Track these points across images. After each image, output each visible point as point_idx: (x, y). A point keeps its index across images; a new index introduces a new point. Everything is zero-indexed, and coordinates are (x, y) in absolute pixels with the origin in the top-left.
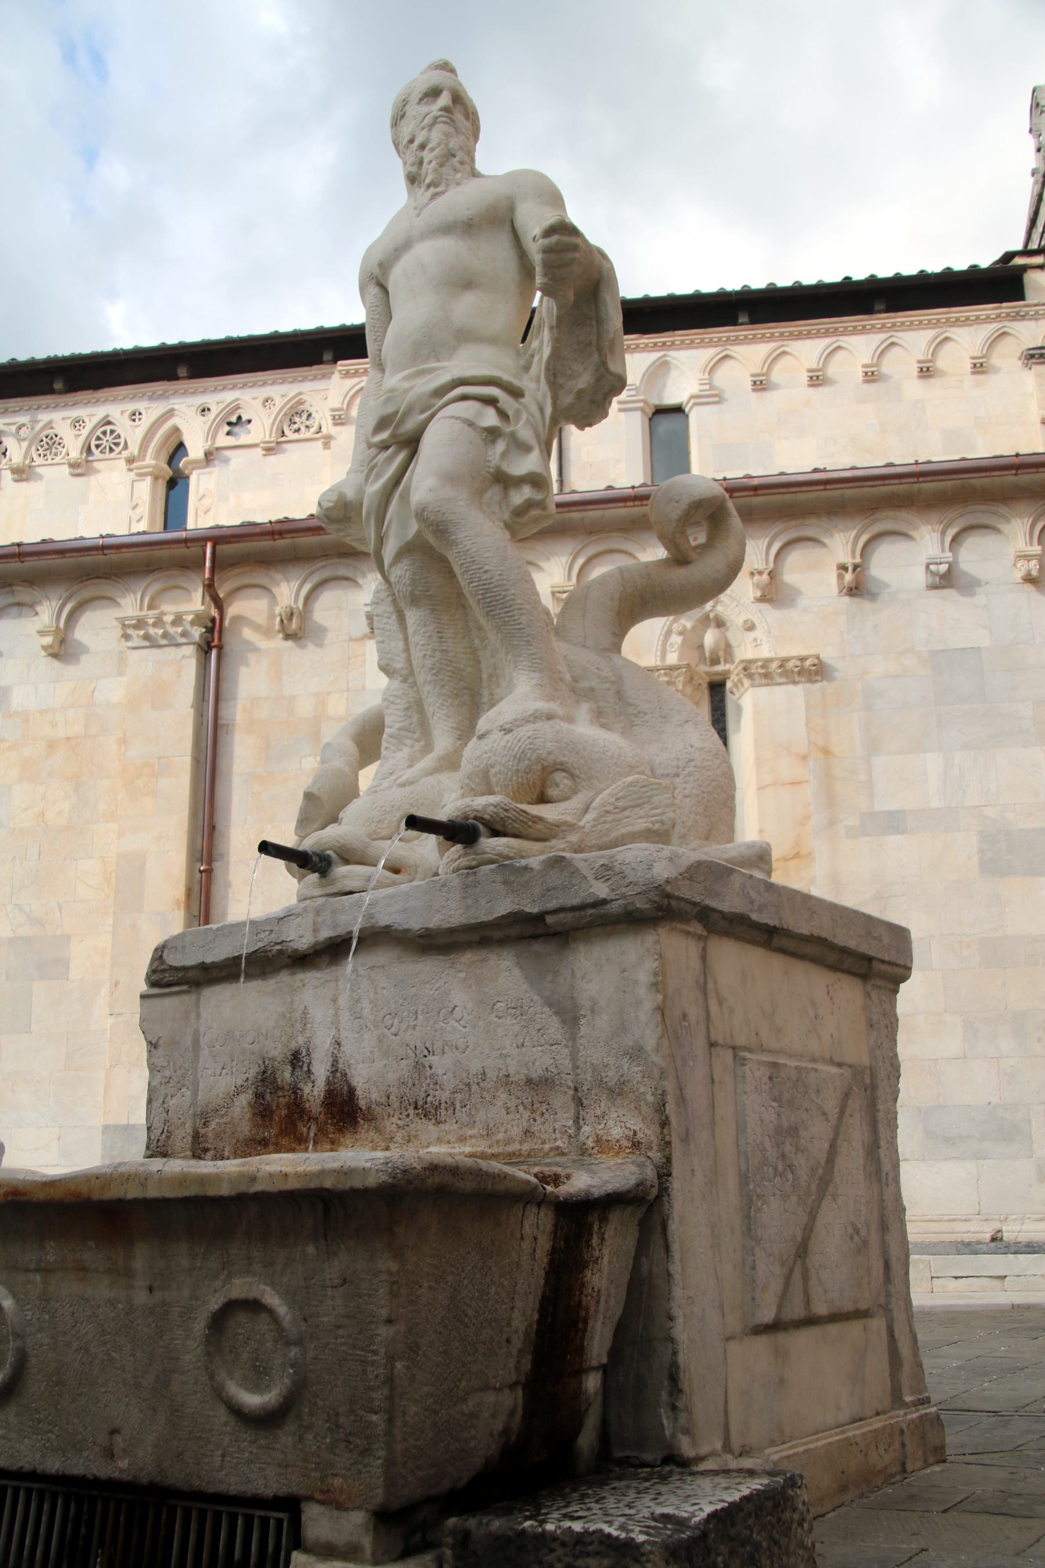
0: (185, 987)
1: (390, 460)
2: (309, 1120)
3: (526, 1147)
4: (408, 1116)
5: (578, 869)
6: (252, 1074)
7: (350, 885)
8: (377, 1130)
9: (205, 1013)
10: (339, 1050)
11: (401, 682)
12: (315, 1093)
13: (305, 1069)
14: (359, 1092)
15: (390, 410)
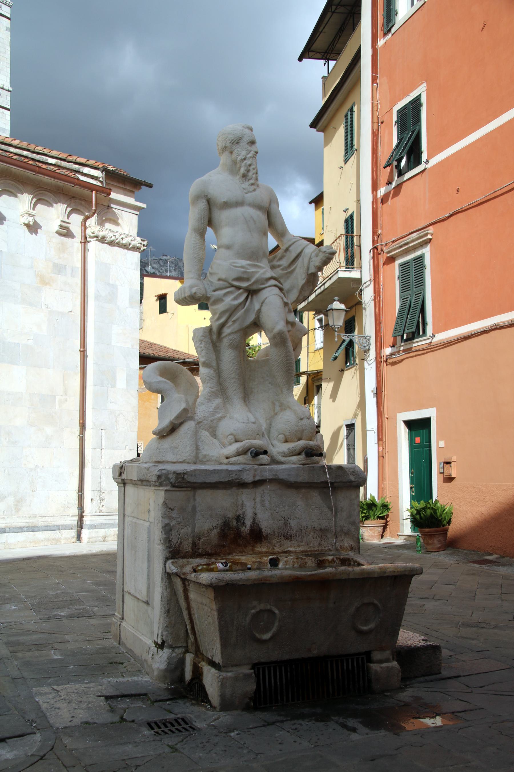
0: (189, 489)
1: (240, 294)
2: (243, 539)
3: (320, 549)
4: (281, 538)
5: (346, 471)
6: (220, 522)
7: (264, 462)
8: (270, 543)
9: (198, 499)
10: (256, 516)
11: (214, 371)
12: (246, 530)
13: (242, 522)
14: (263, 530)
15: (245, 276)
